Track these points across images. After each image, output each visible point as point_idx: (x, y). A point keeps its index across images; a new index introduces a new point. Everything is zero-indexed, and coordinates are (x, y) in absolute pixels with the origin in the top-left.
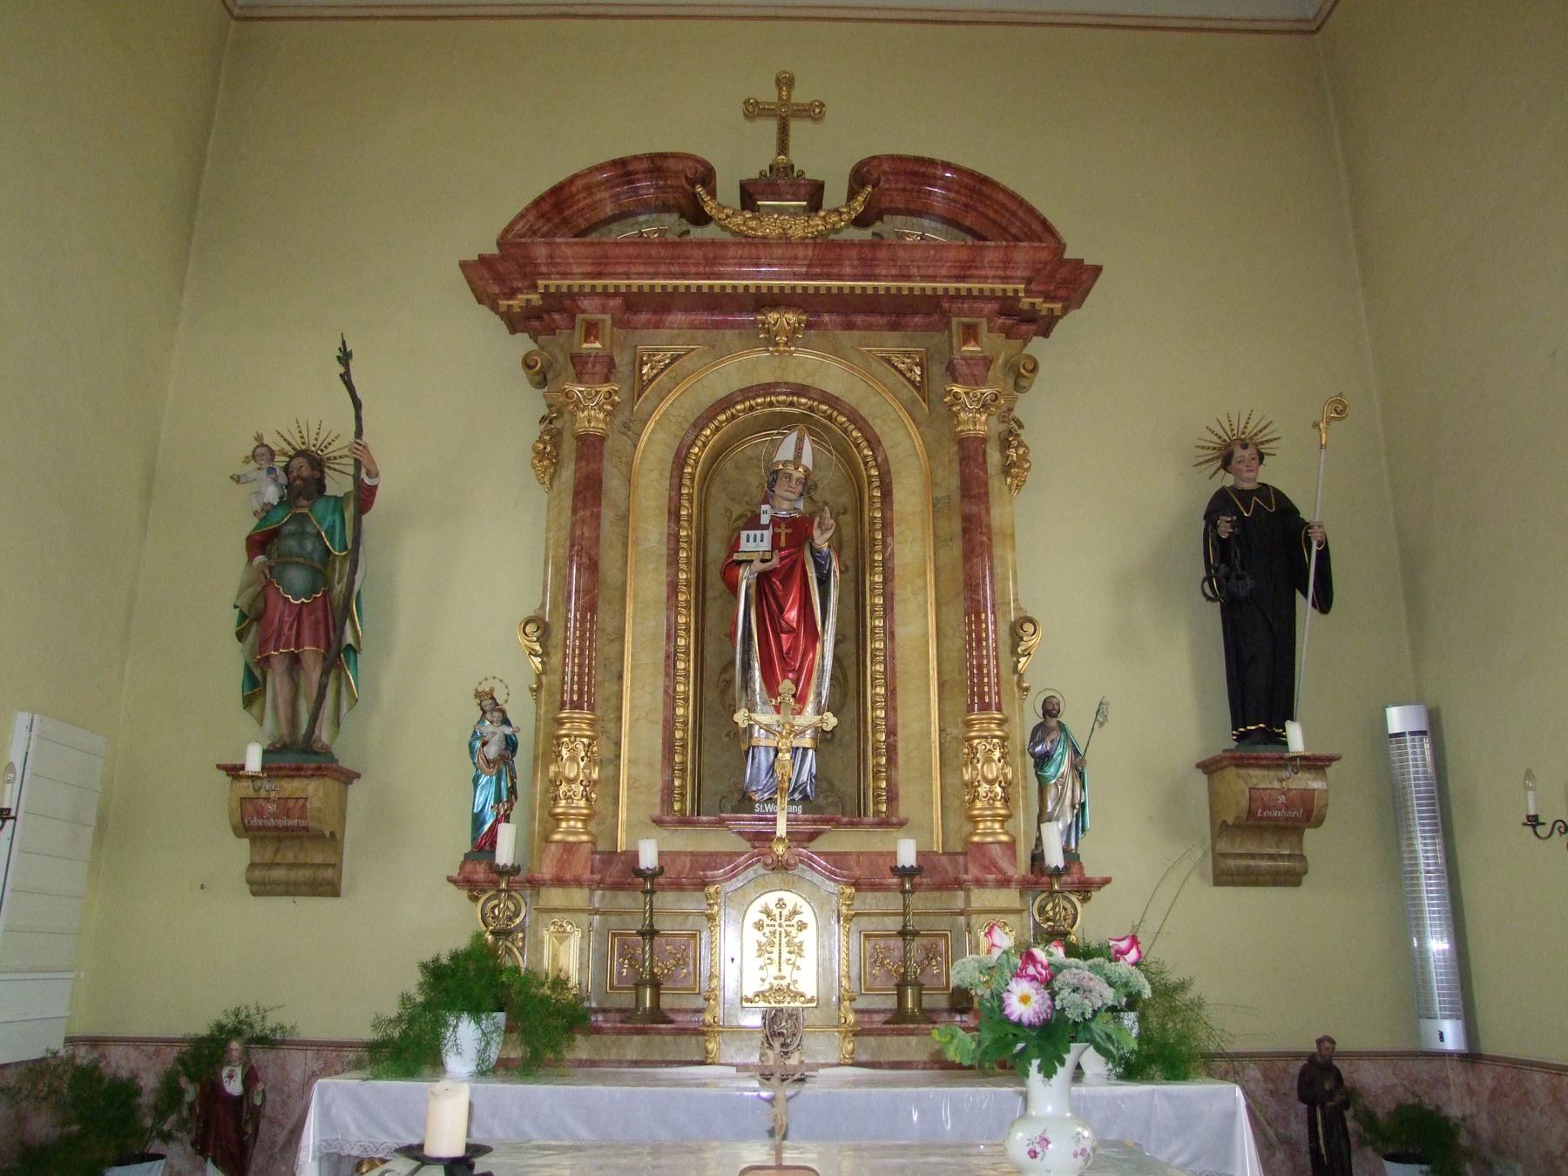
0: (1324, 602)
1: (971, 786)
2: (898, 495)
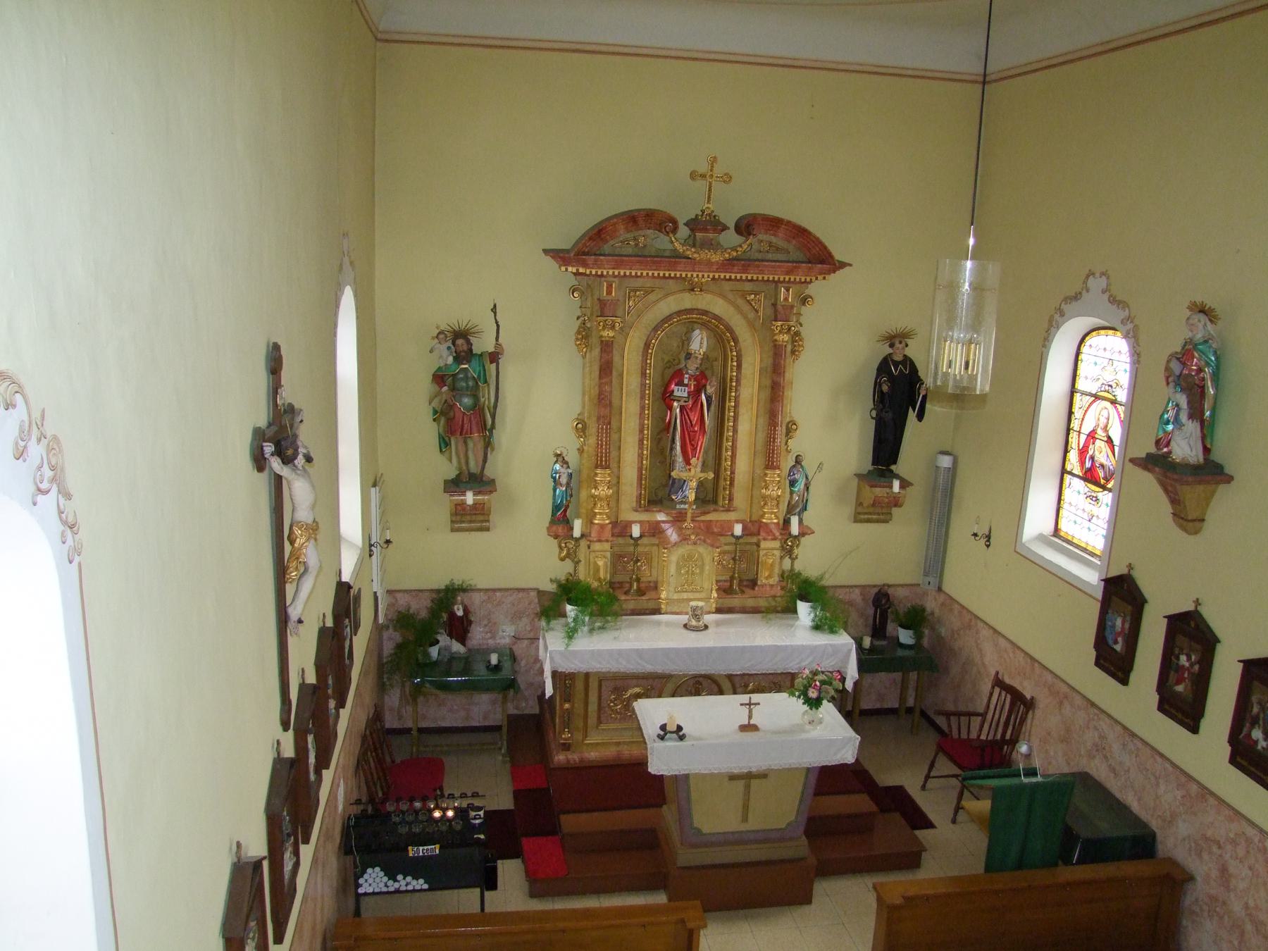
0: (920, 417)
1: (764, 497)
2: (744, 366)
